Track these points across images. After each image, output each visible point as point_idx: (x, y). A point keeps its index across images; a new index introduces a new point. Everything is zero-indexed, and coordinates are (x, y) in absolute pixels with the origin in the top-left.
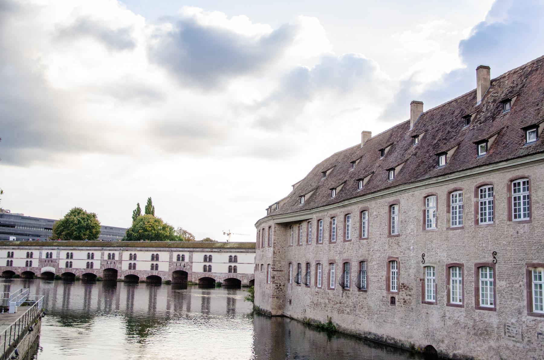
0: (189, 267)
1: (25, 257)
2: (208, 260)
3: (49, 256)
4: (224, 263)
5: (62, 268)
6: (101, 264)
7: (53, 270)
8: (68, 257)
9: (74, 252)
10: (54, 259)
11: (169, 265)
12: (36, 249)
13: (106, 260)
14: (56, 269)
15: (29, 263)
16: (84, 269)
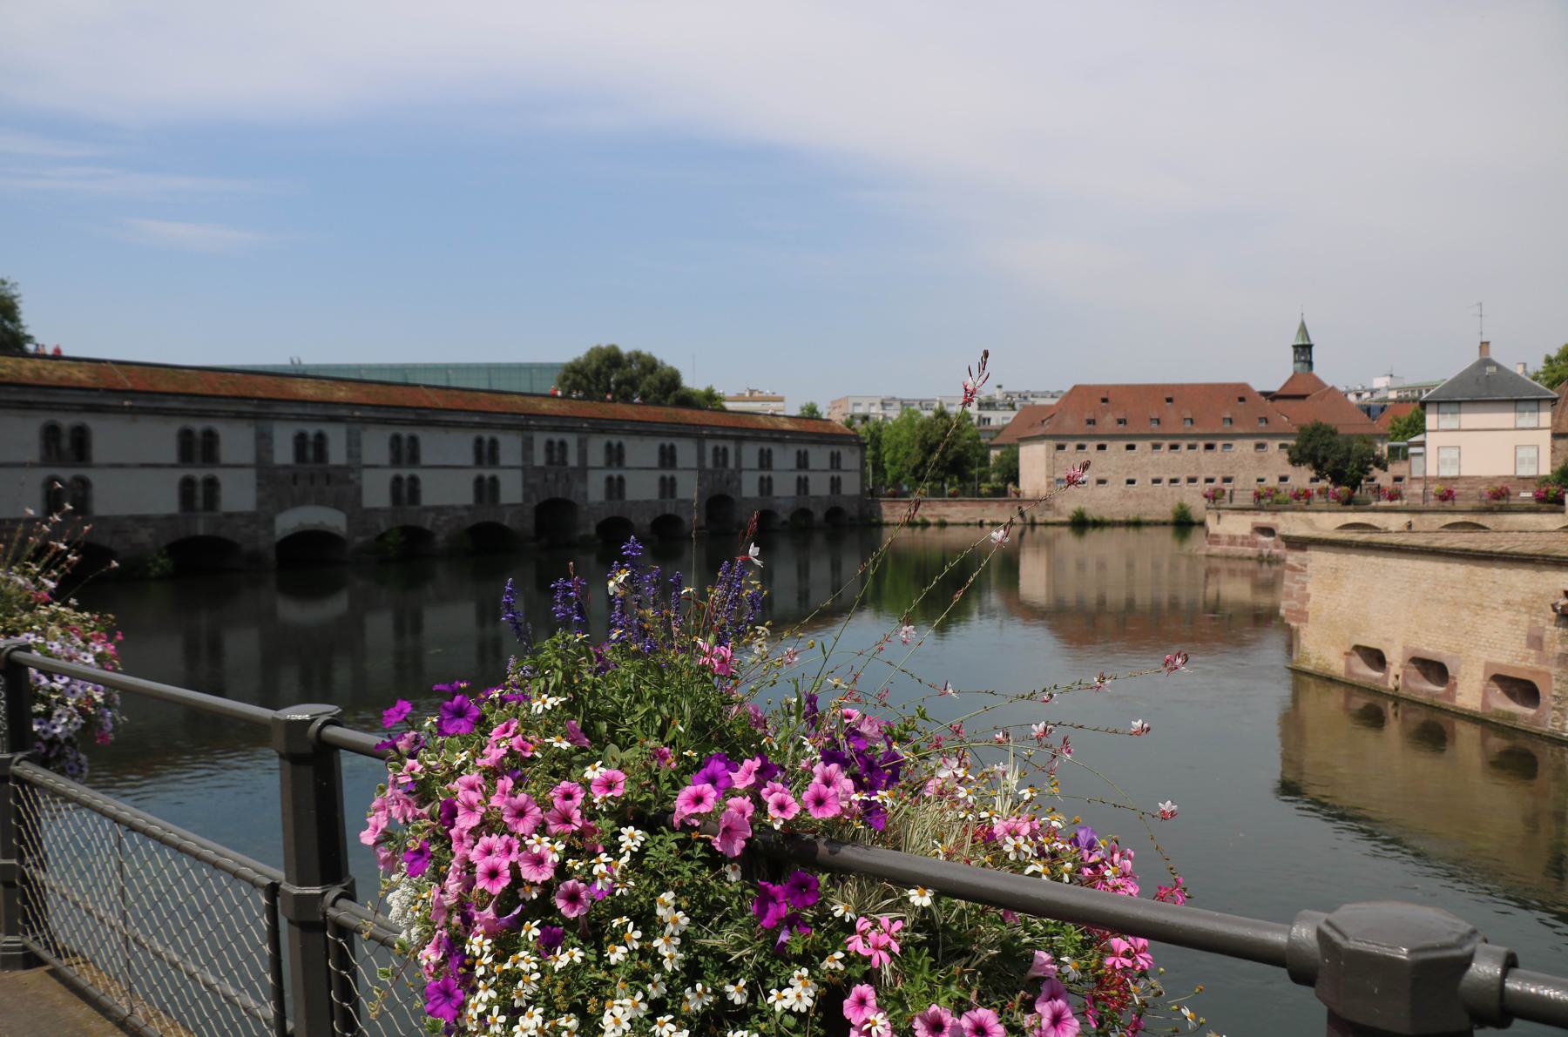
0: (735, 484)
1: (173, 457)
2: (765, 462)
3: (310, 453)
4: (791, 470)
5: (376, 510)
6: (525, 485)
7: (331, 519)
8: (396, 460)
9: (421, 433)
10: (338, 467)
11: (699, 478)
12: (239, 416)
13: (541, 468)
14: (349, 518)
15: (199, 492)
16: (467, 508)
